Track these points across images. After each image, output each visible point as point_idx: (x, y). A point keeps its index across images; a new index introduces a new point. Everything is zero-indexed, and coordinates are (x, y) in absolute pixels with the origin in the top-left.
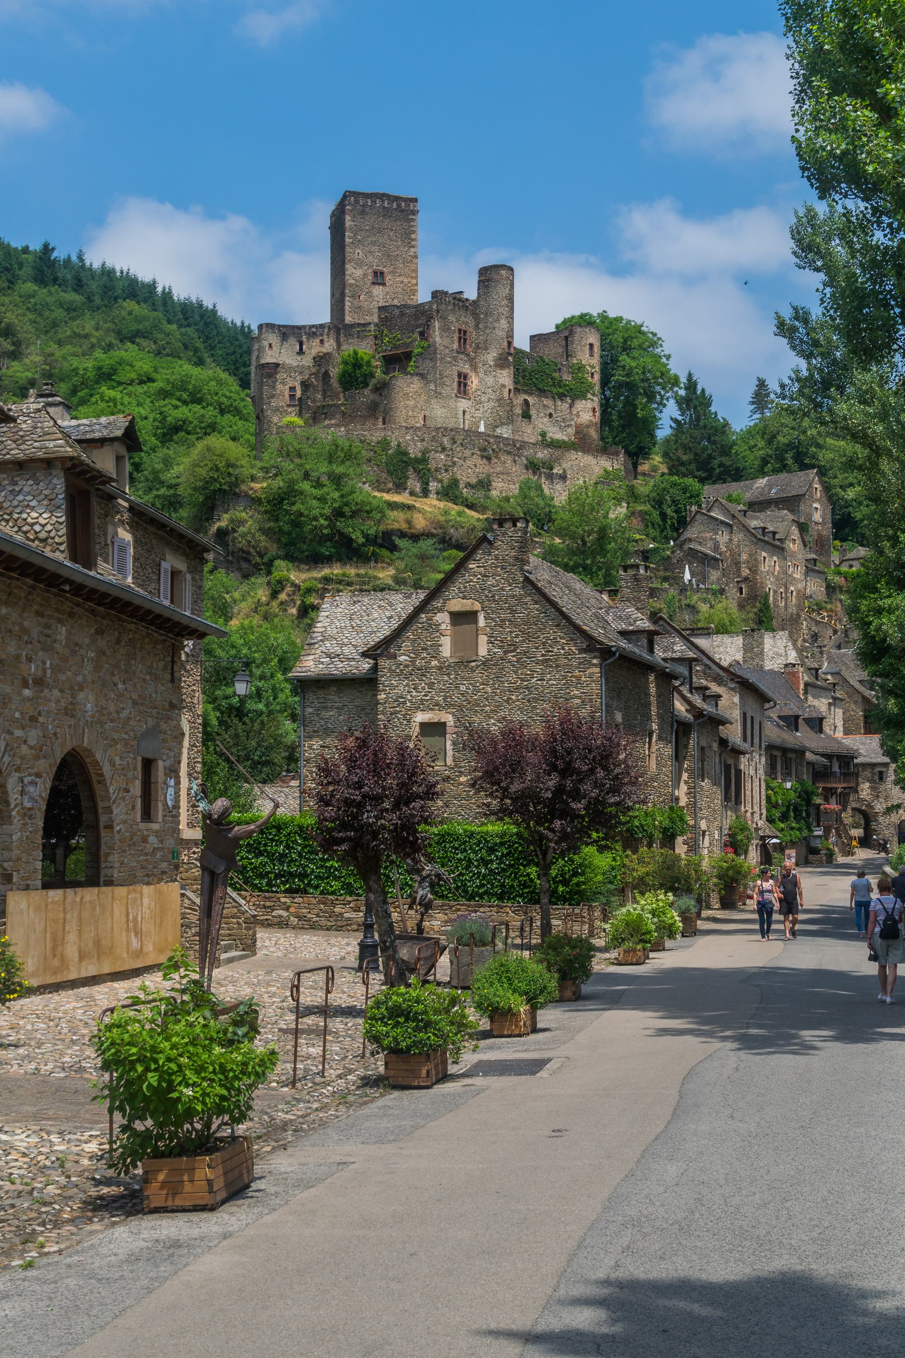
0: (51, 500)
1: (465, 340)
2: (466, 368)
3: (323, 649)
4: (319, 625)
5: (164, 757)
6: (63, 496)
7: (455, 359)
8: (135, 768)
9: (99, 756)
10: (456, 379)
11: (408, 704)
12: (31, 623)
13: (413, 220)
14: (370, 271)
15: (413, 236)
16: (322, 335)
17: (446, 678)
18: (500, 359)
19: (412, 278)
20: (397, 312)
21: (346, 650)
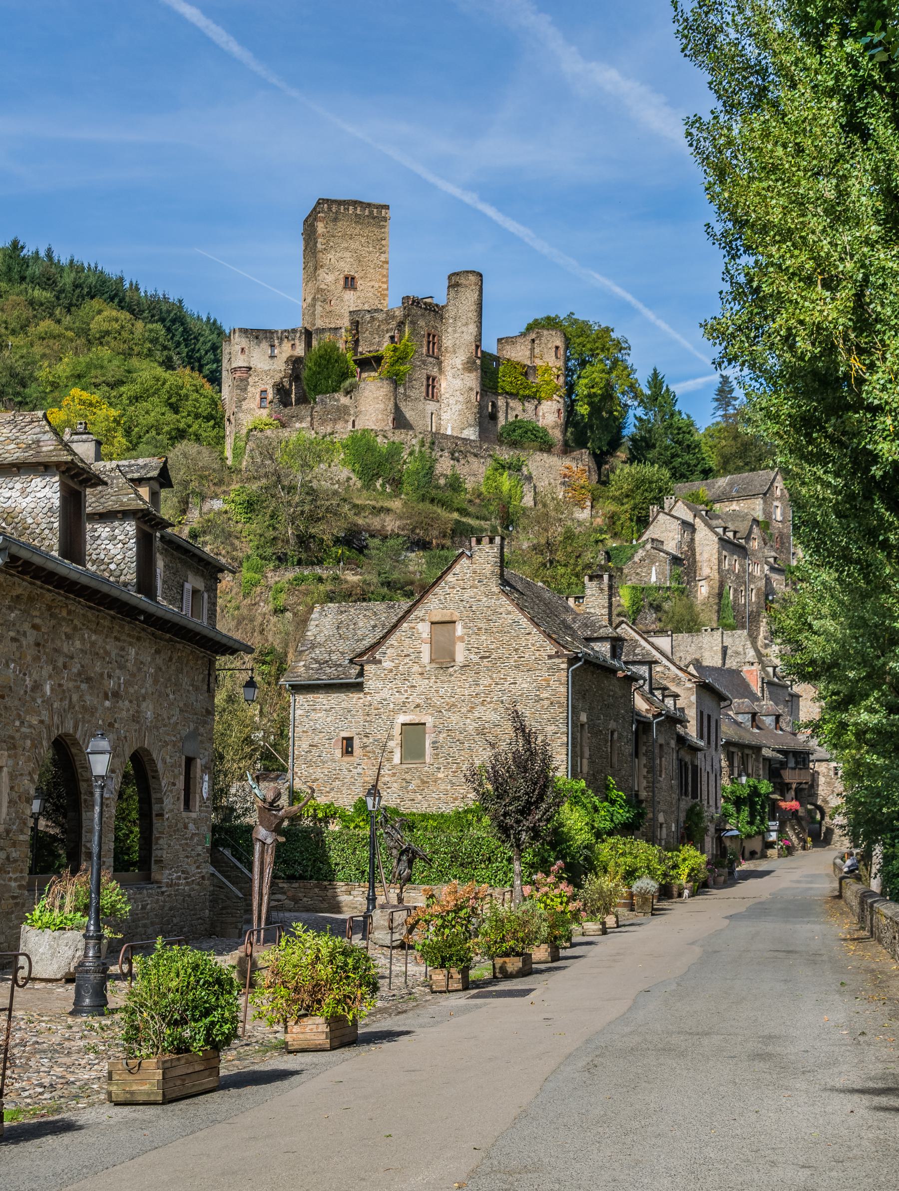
0: (124, 544)
1: (434, 344)
2: (435, 372)
3: (313, 655)
4: (309, 633)
5: (201, 756)
6: (134, 540)
7: (424, 362)
8: (180, 766)
9: (154, 756)
10: (425, 383)
11: (392, 706)
12: (112, 647)
13: (384, 227)
14: (342, 276)
15: (383, 242)
16: (294, 339)
17: (427, 681)
18: (468, 362)
19: (383, 282)
20: (368, 316)
21: (334, 657)
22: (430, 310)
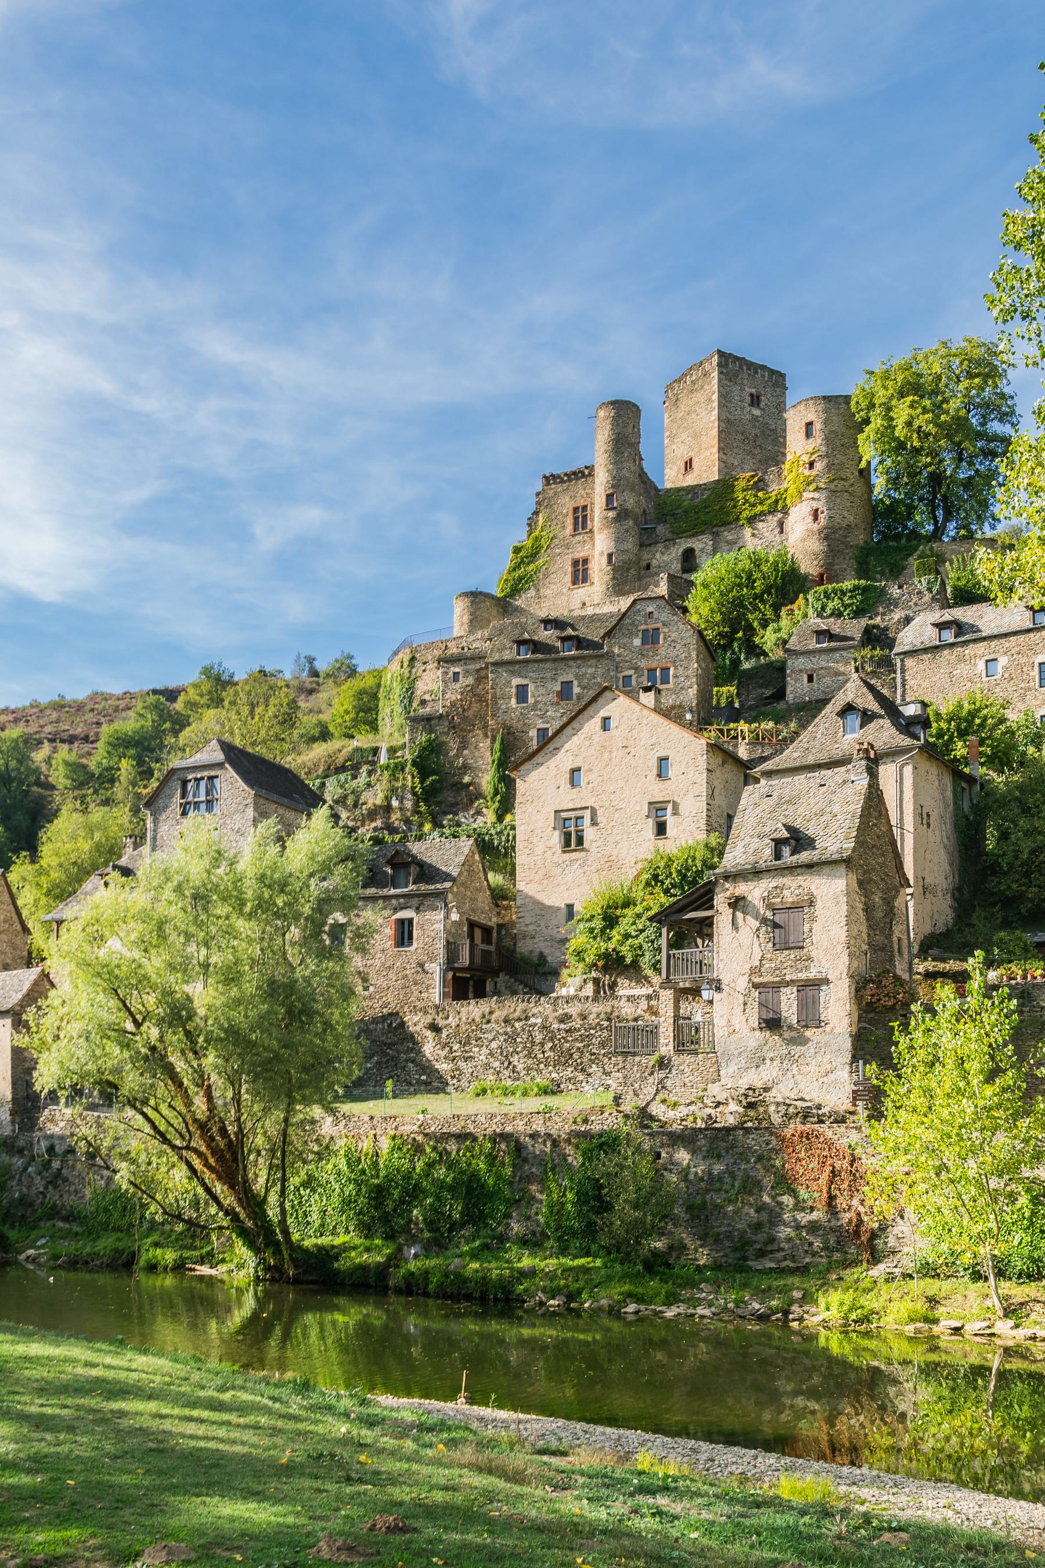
1: (585, 517)
10: (569, 569)
22: (577, 479)
